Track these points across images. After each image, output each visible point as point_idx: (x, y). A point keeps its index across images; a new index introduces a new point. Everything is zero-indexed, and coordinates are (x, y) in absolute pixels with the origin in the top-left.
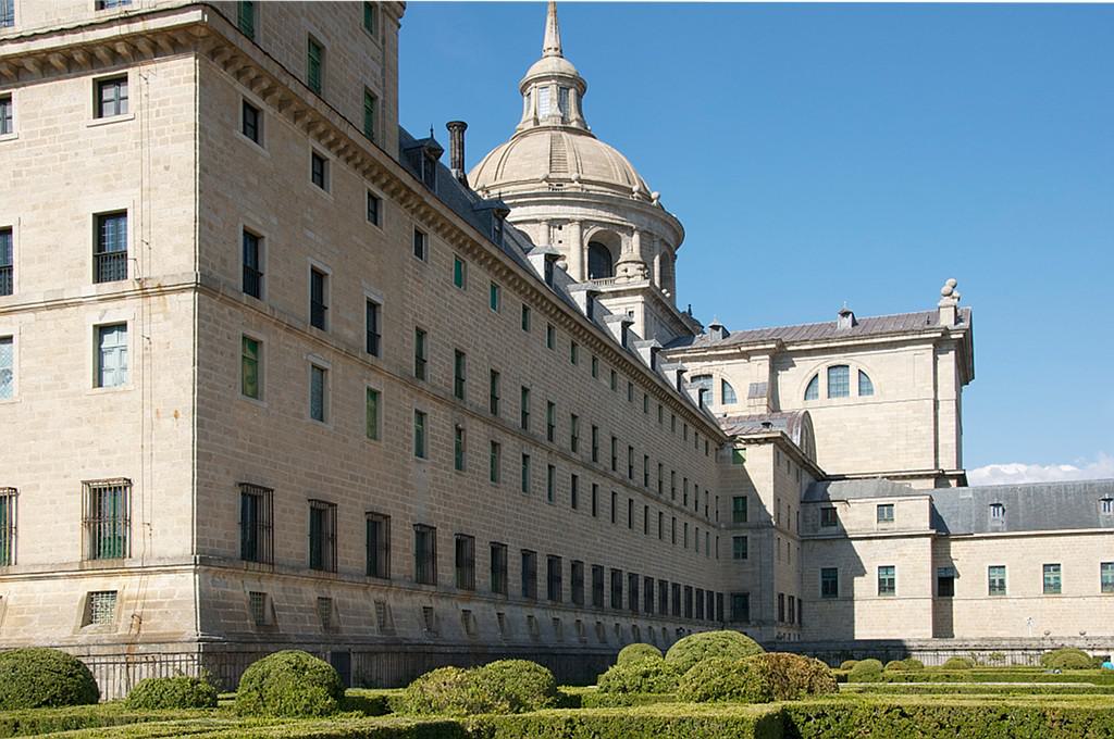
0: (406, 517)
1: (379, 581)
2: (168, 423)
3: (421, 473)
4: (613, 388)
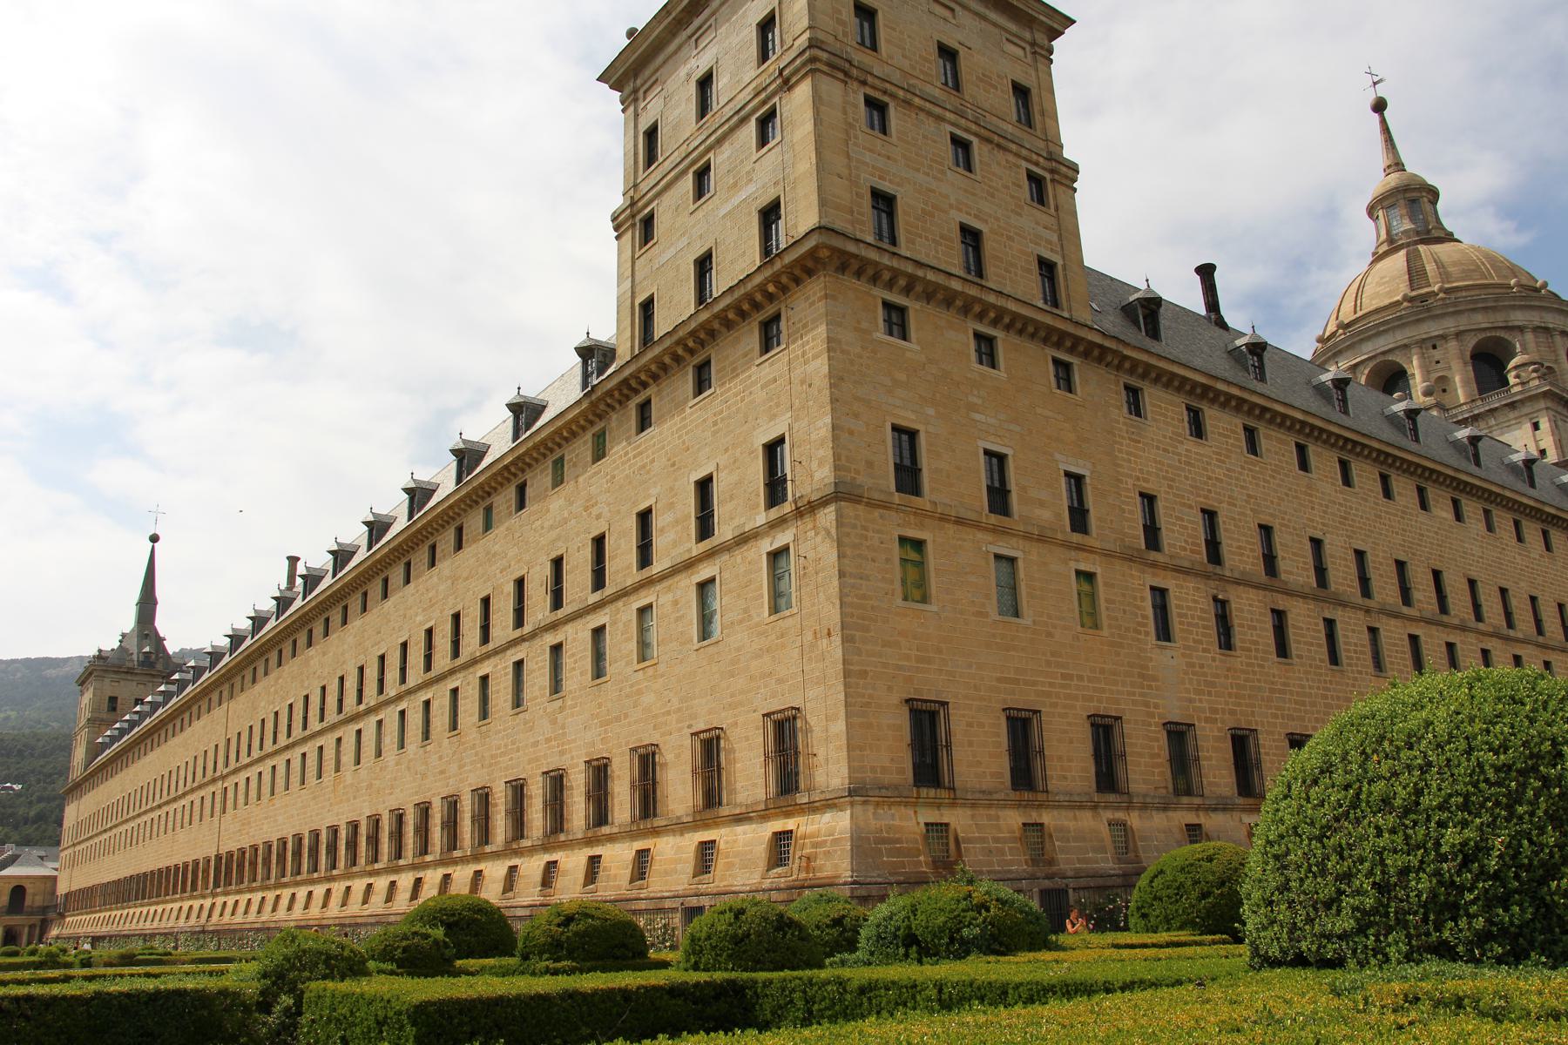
0: (1152, 715)
1: (1112, 797)
3: (1166, 660)
4: (1459, 517)
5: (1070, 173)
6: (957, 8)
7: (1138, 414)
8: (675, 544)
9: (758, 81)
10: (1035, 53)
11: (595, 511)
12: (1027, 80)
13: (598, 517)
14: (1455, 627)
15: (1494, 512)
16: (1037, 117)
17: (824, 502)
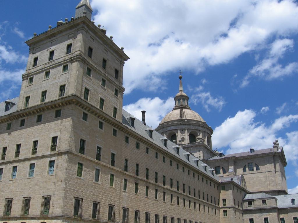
2: (60, 183)
4: (183, 171)
5: (123, 90)
6: (108, 51)
7: (127, 143)
8: (26, 154)
9: (65, 58)
10: (121, 63)
11: (5, 141)
12: (119, 69)
13: (6, 143)
14: (179, 194)
15: (190, 171)
16: (119, 77)
17: (65, 153)
